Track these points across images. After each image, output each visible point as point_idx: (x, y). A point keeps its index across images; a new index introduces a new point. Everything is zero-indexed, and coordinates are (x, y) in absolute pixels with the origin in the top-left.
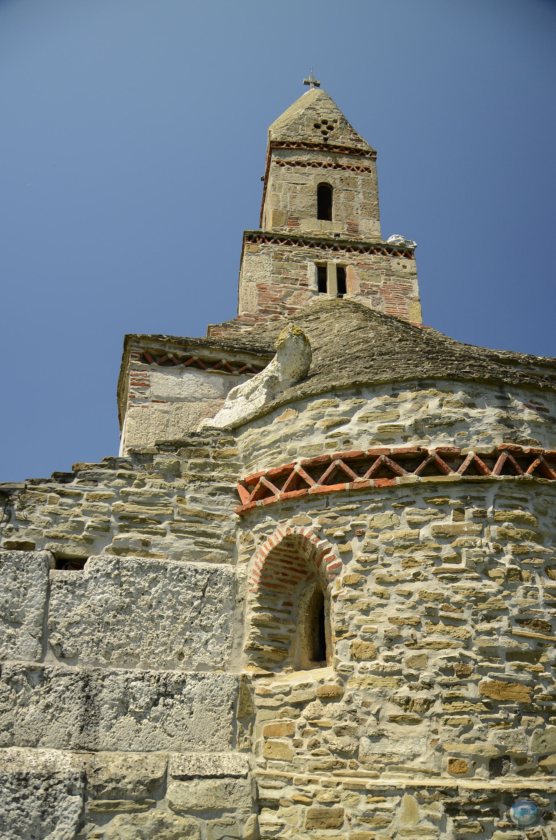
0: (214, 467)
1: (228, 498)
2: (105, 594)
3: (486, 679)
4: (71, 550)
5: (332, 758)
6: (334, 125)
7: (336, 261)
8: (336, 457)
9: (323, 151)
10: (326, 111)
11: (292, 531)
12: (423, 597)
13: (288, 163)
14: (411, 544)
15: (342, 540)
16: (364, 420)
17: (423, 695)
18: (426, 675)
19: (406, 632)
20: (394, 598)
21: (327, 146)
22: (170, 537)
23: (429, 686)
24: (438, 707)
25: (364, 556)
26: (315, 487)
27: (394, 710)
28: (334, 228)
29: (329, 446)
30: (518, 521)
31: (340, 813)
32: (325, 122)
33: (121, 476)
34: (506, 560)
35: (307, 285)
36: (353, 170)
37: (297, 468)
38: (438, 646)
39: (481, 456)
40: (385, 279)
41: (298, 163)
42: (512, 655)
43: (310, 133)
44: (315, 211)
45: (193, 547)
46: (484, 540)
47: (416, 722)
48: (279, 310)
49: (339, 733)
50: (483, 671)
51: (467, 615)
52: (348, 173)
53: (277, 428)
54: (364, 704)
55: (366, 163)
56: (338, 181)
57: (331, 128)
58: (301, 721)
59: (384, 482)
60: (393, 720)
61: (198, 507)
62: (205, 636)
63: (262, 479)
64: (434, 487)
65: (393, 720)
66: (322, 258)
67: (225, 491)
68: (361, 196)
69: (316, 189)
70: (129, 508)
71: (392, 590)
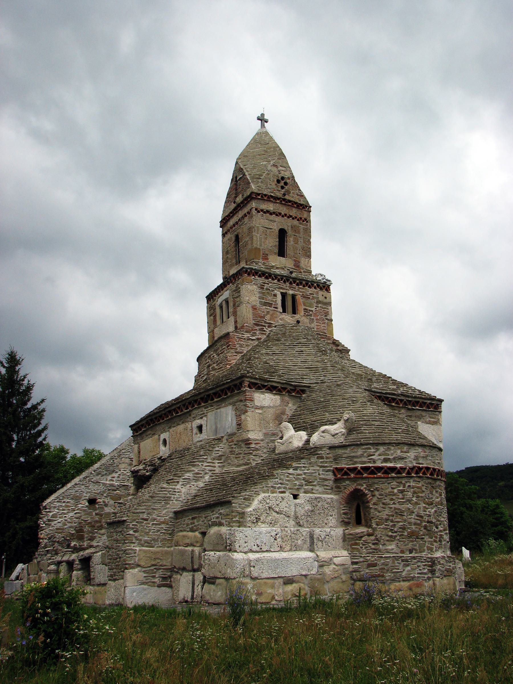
0: (326, 462)
2: (308, 507)
5: (371, 551)
6: (288, 181)
7: (291, 292)
8: (372, 466)
9: (282, 204)
10: (283, 169)
11: (357, 487)
12: (395, 509)
13: (262, 210)
16: (379, 455)
17: (395, 534)
19: (391, 518)
21: (284, 200)
22: (317, 488)
23: (396, 532)
24: (398, 538)
27: (388, 538)
30: (418, 487)
31: (376, 563)
32: (283, 178)
34: (414, 499)
35: (277, 308)
36: (298, 220)
37: (359, 468)
38: (399, 522)
39: (410, 468)
40: (316, 306)
41: (268, 212)
42: (415, 524)
43: (275, 187)
44: (276, 250)
45: (324, 490)
46: (410, 493)
47: (393, 541)
48: (263, 324)
49: (374, 544)
50: (409, 528)
51: (405, 514)
52: (295, 222)
54: (381, 537)
56: (290, 228)
57: (286, 184)
58: (362, 542)
59: (385, 475)
60: (388, 541)
61: (323, 477)
62: (331, 518)
63: (345, 469)
64: (398, 478)
65: (388, 541)
67: (329, 470)
68: (302, 241)
69: (278, 234)
70: (307, 478)
71: (387, 506)
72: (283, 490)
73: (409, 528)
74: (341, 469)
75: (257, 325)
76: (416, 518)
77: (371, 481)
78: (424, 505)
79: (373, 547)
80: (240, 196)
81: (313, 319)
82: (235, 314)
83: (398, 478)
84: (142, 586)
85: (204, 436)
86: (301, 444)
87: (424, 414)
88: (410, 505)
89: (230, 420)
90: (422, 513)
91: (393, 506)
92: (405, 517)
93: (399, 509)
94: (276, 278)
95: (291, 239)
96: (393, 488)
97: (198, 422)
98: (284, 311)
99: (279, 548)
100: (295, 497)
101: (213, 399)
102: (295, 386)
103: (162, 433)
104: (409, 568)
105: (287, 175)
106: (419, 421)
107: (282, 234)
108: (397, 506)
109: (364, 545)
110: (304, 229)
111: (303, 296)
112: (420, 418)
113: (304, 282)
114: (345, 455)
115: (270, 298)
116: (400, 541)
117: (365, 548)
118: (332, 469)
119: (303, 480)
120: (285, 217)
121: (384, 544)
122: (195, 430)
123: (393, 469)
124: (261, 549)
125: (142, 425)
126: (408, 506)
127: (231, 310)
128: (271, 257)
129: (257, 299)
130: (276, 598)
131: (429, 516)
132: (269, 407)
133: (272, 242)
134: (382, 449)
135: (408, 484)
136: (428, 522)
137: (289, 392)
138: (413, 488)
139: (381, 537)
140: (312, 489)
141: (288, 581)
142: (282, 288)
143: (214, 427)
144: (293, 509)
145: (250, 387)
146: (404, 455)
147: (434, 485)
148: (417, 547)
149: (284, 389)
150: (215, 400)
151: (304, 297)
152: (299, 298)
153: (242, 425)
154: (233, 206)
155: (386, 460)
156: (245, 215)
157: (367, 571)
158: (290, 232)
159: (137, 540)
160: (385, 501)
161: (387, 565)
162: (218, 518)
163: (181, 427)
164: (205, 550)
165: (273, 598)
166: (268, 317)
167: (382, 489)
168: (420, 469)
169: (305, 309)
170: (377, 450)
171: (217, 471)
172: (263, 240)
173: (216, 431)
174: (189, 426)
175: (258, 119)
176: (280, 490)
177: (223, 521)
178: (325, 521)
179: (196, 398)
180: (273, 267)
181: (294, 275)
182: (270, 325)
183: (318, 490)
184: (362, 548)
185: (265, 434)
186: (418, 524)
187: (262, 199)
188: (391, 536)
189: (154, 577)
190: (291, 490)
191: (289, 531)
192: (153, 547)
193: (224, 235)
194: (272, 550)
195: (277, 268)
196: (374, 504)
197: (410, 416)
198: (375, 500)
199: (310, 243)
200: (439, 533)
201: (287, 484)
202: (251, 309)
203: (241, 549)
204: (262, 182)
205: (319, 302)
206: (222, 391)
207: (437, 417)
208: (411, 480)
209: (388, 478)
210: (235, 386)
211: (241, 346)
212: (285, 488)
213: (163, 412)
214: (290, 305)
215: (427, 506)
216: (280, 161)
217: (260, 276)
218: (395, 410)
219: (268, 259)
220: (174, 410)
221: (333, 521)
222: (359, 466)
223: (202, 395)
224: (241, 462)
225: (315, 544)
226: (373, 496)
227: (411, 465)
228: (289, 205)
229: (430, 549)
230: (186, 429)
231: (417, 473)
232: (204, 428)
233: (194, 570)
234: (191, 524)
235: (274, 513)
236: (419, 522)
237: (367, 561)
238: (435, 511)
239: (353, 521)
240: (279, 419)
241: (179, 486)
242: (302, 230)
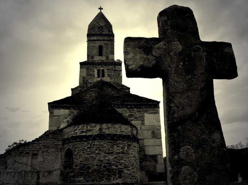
0: (59, 136)
1: (61, 142)
3: (92, 169)
5: (72, 181)
7: (102, 69)
10: (101, 23)
12: (85, 157)
13: (91, 40)
15: (75, 149)
19: (82, 163)
20: (81, 158)
22: (51, 149)
23: (84, 170)
24: (85, 173)
25: (78, 152)
27: (80, 174)
28: (103, 58)
29: (74, 134)
30: (100, 145)
32: (101, 27)
33: (43, 140)
34: (97, 152)
42: (97, 165)
44: (98, 54)
47: (82, 175)
49: (73, 178)
52: (107, 42)
55: (111, 38)
59: (81, 140)
61: (56, 144)
62: (56, 164)
65: (80, 175)
66: (98, 68)
68: (110, 48)
71: (81, 156)
72: (28, 152)
73: (92, 168)
76: (98, 161)
77: (74, 143)
78: (105, 154)
79: (72, 179)
81: (112, 78)
83: (88, 141)
87: (148, 109)
88: (94, 155)
90: (102, 159)
92: (90, 162)
93: (87, 157)
95: (105, 49)
96: (84, 146)
99: (16, 182)
106: (146, 113)
107: (101, 48)
108: (86, 156)
109: (69, 178)
111: (107, 69)
112: (146, 111)
113: (108, 64)
115: (91, 73)
116: (86, 175)
117: (70, 179)
118: (62, 139)
119: (42, 146)
120: (102, 41)
121: (78, 177)
124: (3, 183)
126: (92, 155)
128: (95, 57)
129: (85, 74)
132: (62, 115)
133: (96, 51)
134: (80, 126)
135: (93, 143)
136: (107, 163)
138: (96, 145)
139: (76, 173)
140: (47, 150)
142: (97, 68)
144: (31, 161)
146: (92, 128)
147: (115, 143)
149: (72, 106)
152: (105, 71)
155: (82, 132)
158: (104, 46)
160: (80, 154)
167: (79, 147)
169: (108, 74)
170: (78, 127)
172: (91, 51)
175: (99, 9)
176: (26, 152)
178: (52, 166)
180: (96, 61)
182: (91, 83)
183: (51, 150)
184: (68, 179)
186: (99, 165)
188: (81, 173)
190: (33, 152)
191: (24, 173)
194: (10, 183)
196: (76, 155)
198: (76, 153)
199: (114, 49)
200: (118, 170)
201: (32, 149)
202: (82, 79)
204: (91, 30)
205: (115, 70)
207: (156, 110)
209: (82, 141)
212: (29, 151)
215: (107, 155)
216: (100, 21)
218: (130, 109)
219: (94, 58)
225: (40, 179)
226: (75, 151)
227: (96, 133)
228: (103, 36)
235: (17, 164)
236: (100, 164)
242: (110, 44)
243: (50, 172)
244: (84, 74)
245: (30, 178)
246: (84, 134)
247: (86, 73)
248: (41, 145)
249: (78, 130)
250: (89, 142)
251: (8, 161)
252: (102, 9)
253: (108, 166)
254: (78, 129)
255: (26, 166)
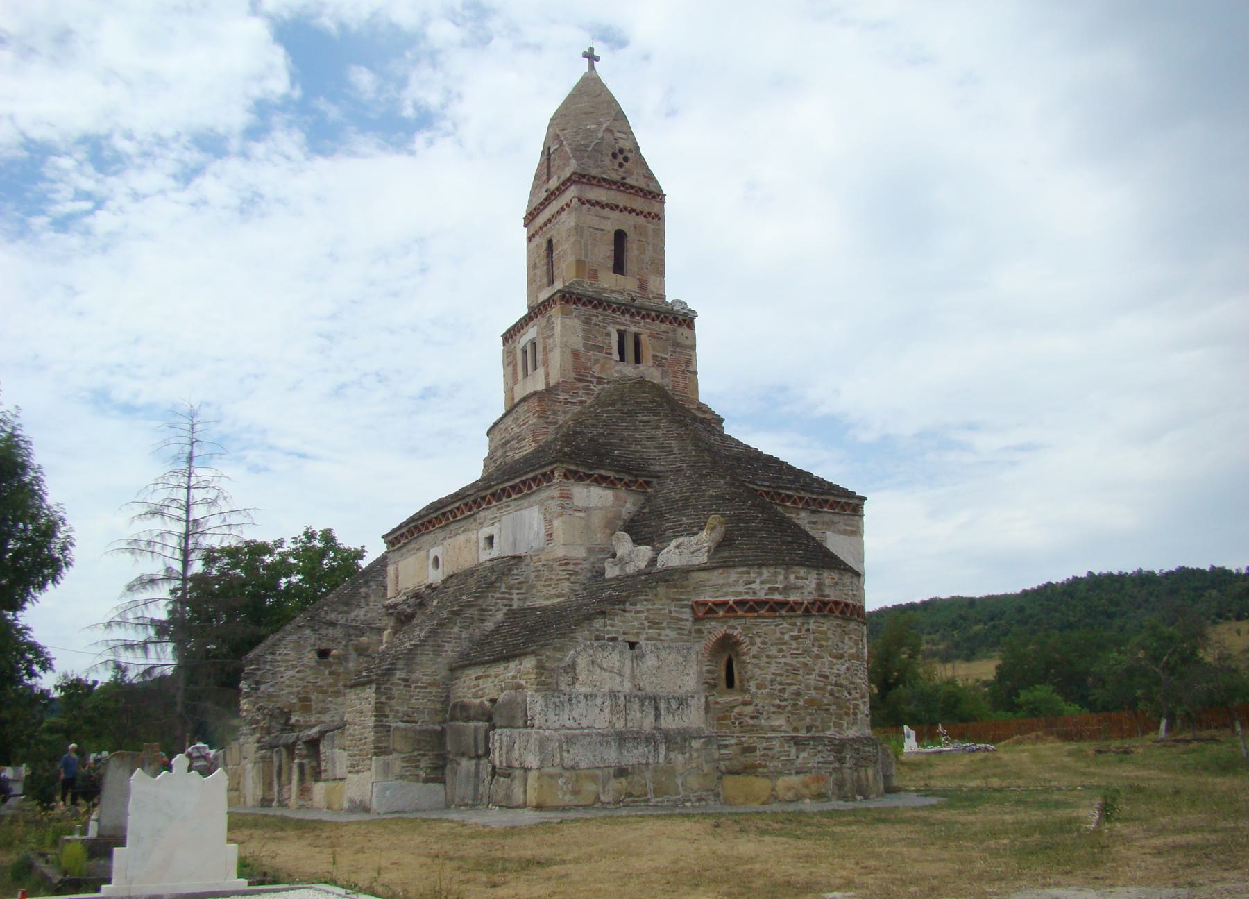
0: (681, 593)
4: (633, 639)
6: (629, 155)
7: (633, 329)
10: (623, 136)
13: (589, 201)
14: (781, 642)
16: (762, 583)
18: (786, 696)
21: (624, 185)
22: (667, 631)
24: (789, 708)
26: (740, 613)
27: (773, 709)
30: (820, 632)
32: (621, 151)
34: (815, 649)
41: (597, 203)
42: (815, 688)
44: (611, 264)
49: (752, 718)
52: (641, 220)
53: (716, 577)
57: (626, 159)
67: (686, 606)
68: (651, 248)
74: (705, 604)
75: (580, 380)
77: (749, 622)
79: (751, 722)
80: (555, 178)
82: (546, 363)
84: (400, 781)
85: (495, 553)
86: (642, 565)
87: (836, 519)
89: (536, 526)
90: (827, 671)
91: (783, 660)
92: (800, 678)
93: (791, 665)
94: (609, 306)
97: (486, 531)
98: (622, 359)
100: (632, 645)
101: (509, 496)
102: (637, 476)
103: (432, 547)
104: (803, 755)
105: (626, 145)
107: (620, 237)
108: (788, 660)
110: (654, 230)
111: (652, 336)
113: (653, 314)
114: (711, 583)
115: (599, 339)
122: (482, 544)
123: (782, 604)
125: (402, 535)
127: (540, 357)
130: (602, 798)
131: (839, 675)
132: (596, 508)
133: (605, 251)
134: (766, 573)
135: (806, 627)
136: (836, 684)
137: (627, 485)
141: (622, 772)
143: (511, 538)
145: (565, 476)
146: (800, 583)
148: (818, 724)
150: (514, 497)
151: (654, 337)
152: (644, 339)
153: (554, 536)
154: (544, 195)
155: (772, 590)
156: (563, 209)
157: (742, 759)
159: (392, 711)
161: (770, 749)
162: (514, 677)
163: (461, 538)
164: (493, 727)
165: (598, 799)
166: (596, 368)
168: (825, 604)
171: (515, 607)
173: (514, 544)
174: (474, 537)
175: (585, 55)
177: (523, 682)
178: (679, 683)
179: (484, 494)
180: (605, 290)
181: (637, 303)
182: (600, 381)
185: (590, 550)
186: (823, 689)
187: (589, 183)
188: (779, 706)
189: (417, 767)
192: (416, 722)
193: (530, 239)
195: (612, 292)
196: (754, 657)
197: (815, 523)
198: (754, 650)
202: (570, 358)
203: (548, 724)
204: (589, 157)
205: (676, 344)
206: (524, 483)
208: (811, 621)
209: (774, 617)
210: (544, 475)
211: (555, 413)
212: (617, 632)
213: (434, 515)
214: (630, 349)
216: (618, 124)
217: (584, 305)
220: (451, 511)
221: (690, 683)
222: (731, 599)
223: (493, 490)
224: (553, 592)
226: (753, 644)
227: (810, 598)
229: (839, 726)
230: (468, 541)
231: (819, 610)
232: (496, 540)
233: (478, 757)
234: (475, 686)
237: (741, 743)
238: (848, 669)
239: (722, 683)
240: (611, 527)
241: (456, 629)
242: (650, 233)
243: (682, 701)
244: (577, 341)
245: (639, 715)
246: (778, 597)
247: (585, 338)
248: (642, 615)
249: (759, 584)
250: (794, 620)
251: (579, 661)
252: (597, 59)
253: (839, 691)
254: (758, 581)
255: (618, 679)
